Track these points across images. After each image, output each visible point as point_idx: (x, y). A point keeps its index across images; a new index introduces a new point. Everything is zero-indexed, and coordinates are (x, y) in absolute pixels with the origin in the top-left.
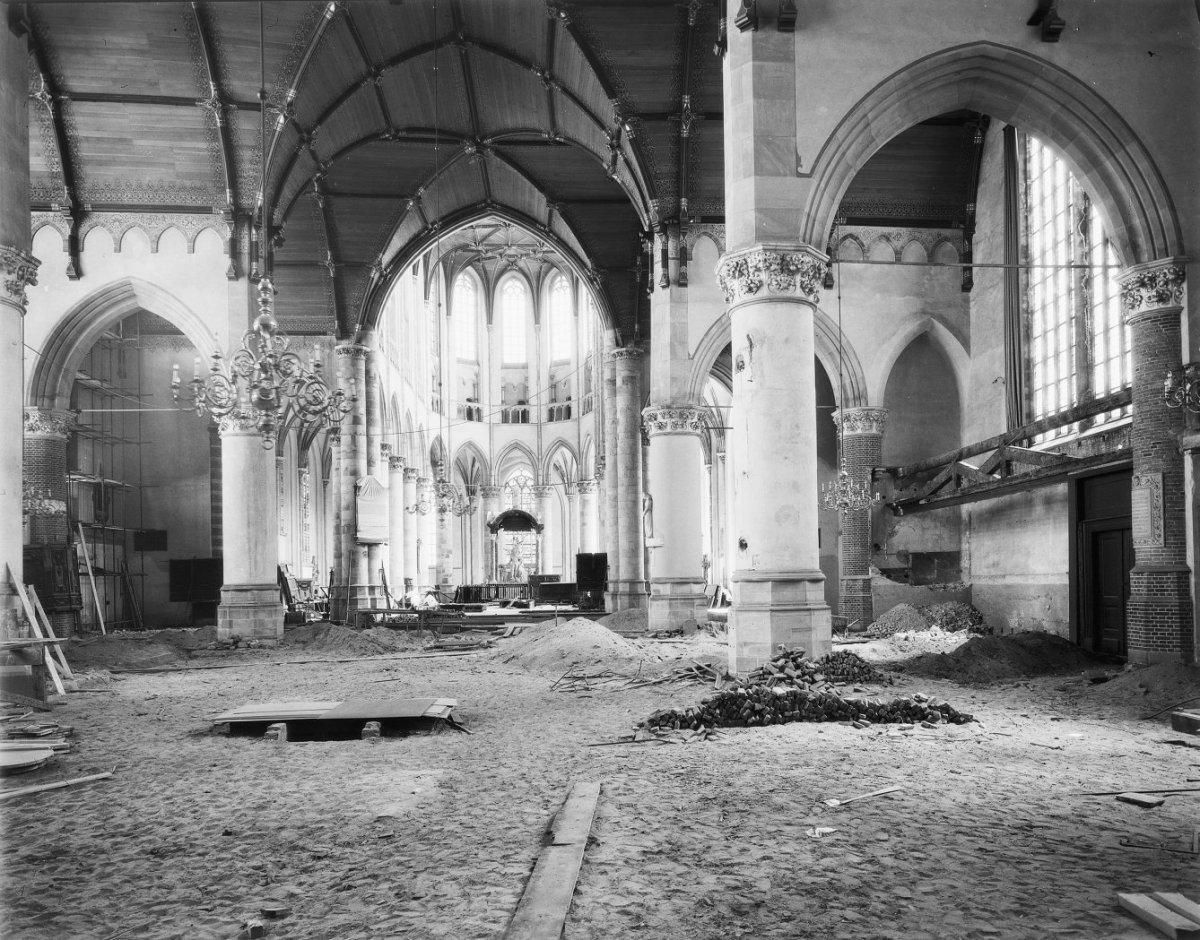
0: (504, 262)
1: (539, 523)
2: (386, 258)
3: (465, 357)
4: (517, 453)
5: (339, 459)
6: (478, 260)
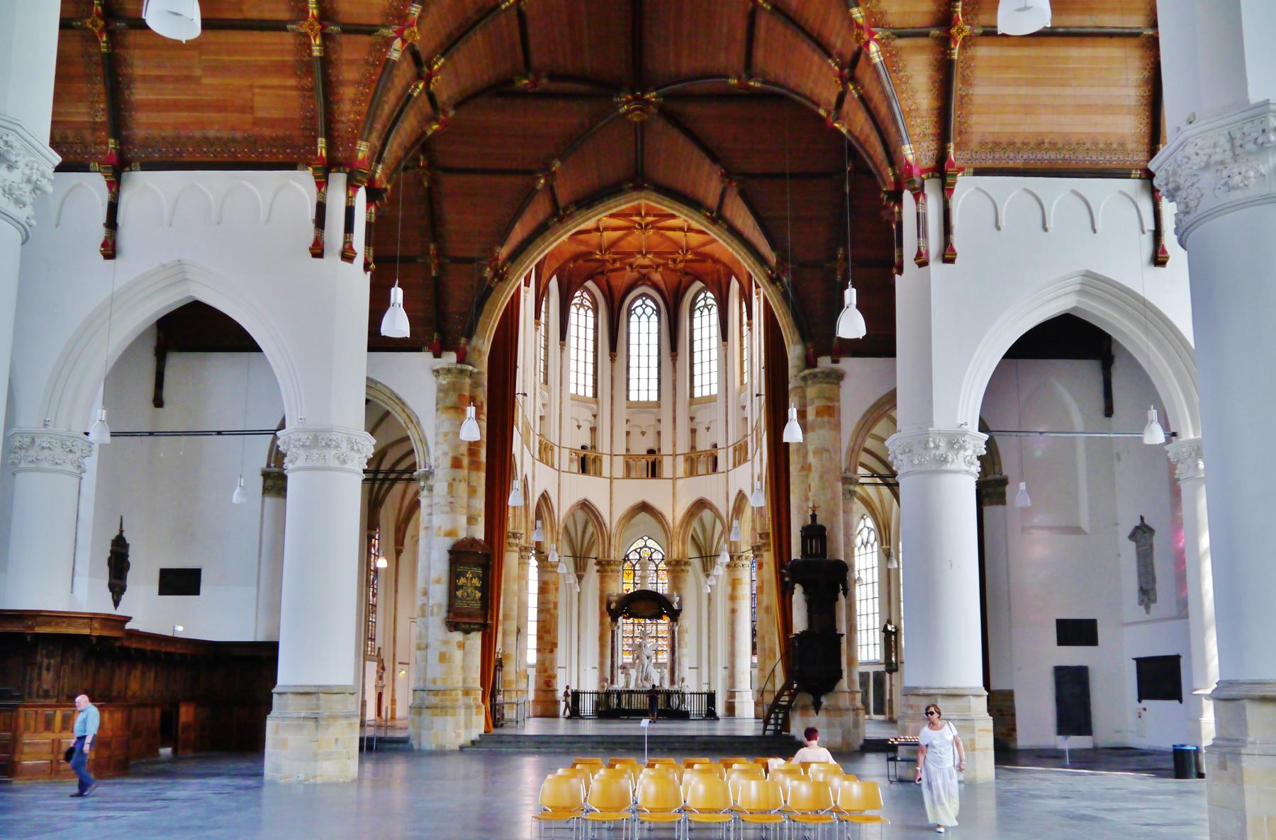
0: (635, 274)
1: (675, 606)
2: (504, 252)
3: (581, 393)
4: (644, 516)
5: (430, 514)
6: (602, 273)
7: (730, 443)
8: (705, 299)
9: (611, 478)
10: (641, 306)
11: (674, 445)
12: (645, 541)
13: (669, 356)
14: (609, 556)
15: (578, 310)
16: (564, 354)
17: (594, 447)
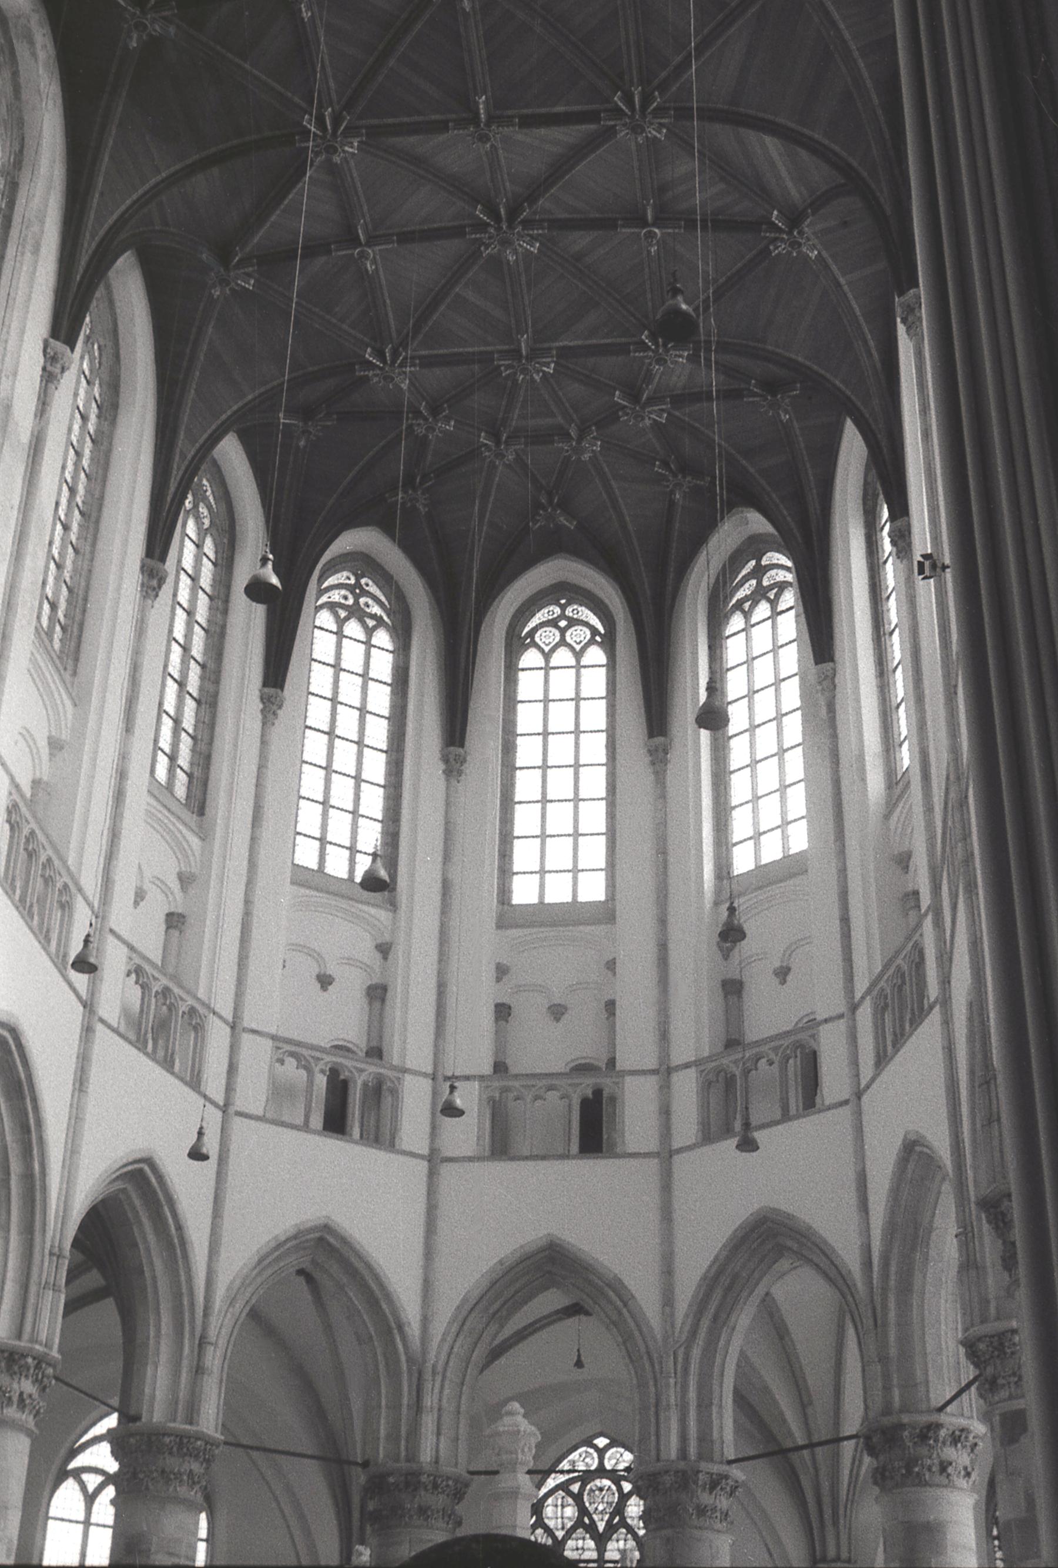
7: (861, 985)
8: (759, 572)
9: (435, 1160)
10: (553, 623)
11: (664, 1036)
12: (601, 1452)
13: (643, 751)
14: (412, 1456)
15: (341, 623)
16: (277, 732)
17: (376, 1052)
